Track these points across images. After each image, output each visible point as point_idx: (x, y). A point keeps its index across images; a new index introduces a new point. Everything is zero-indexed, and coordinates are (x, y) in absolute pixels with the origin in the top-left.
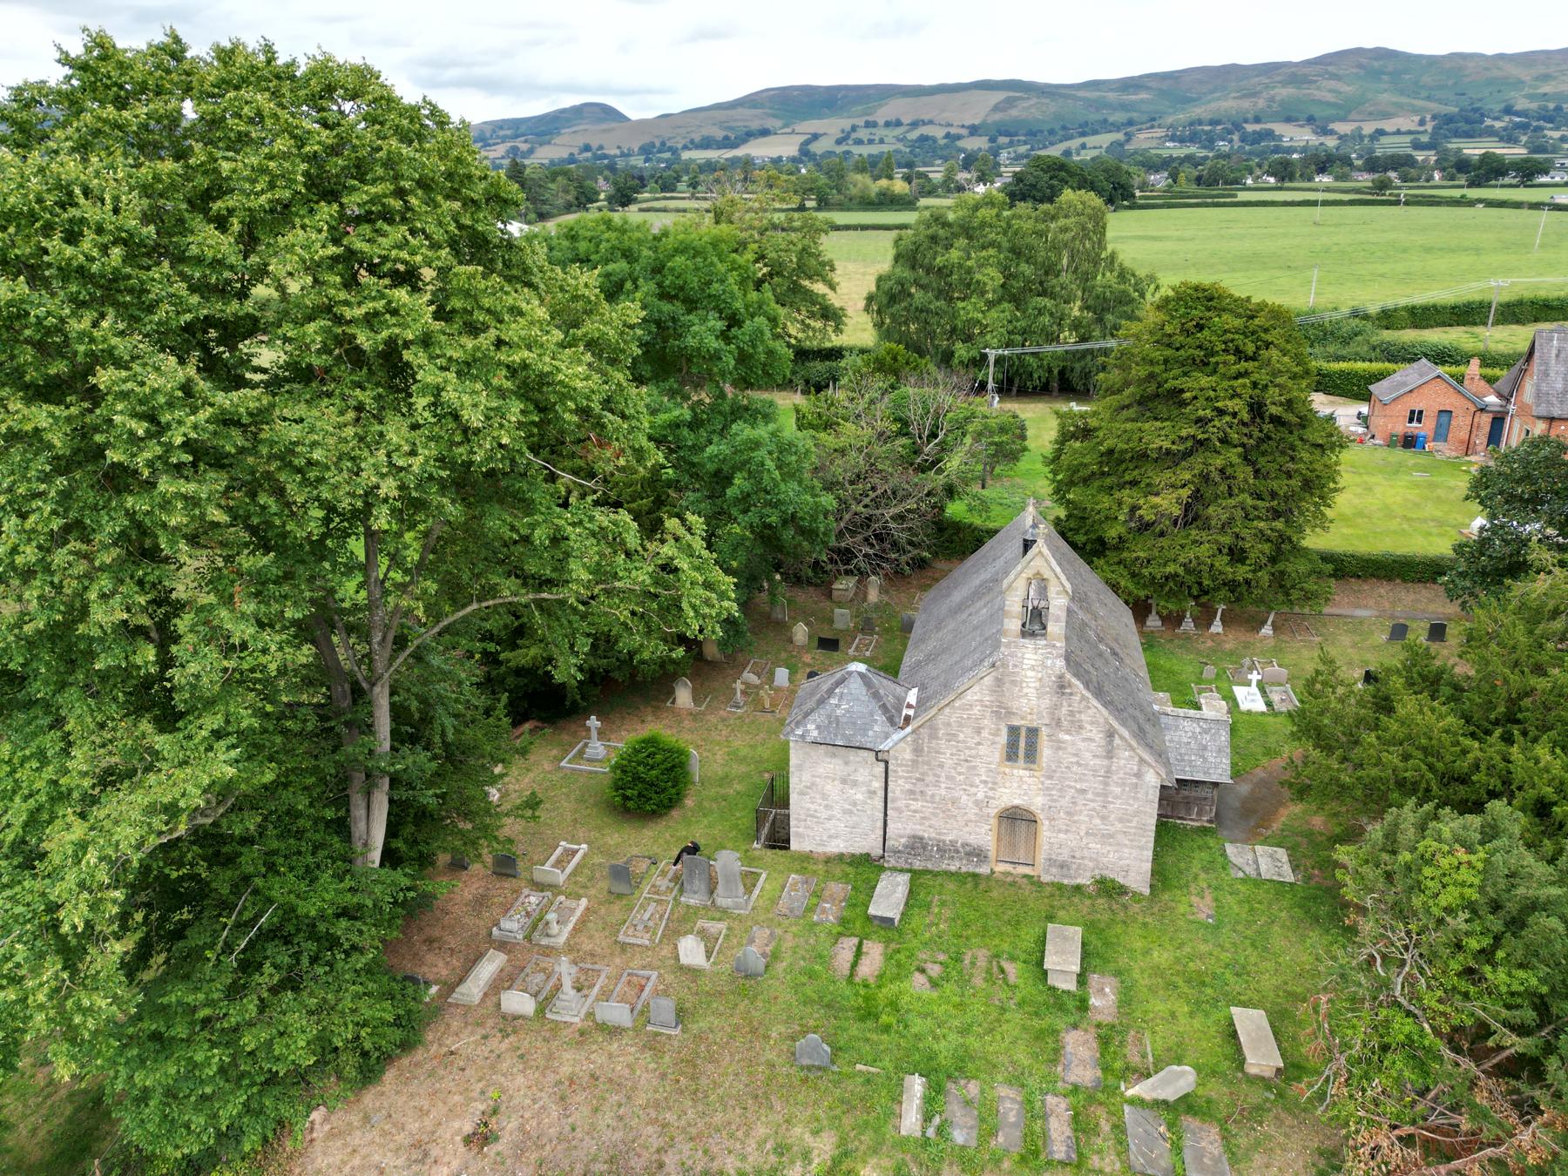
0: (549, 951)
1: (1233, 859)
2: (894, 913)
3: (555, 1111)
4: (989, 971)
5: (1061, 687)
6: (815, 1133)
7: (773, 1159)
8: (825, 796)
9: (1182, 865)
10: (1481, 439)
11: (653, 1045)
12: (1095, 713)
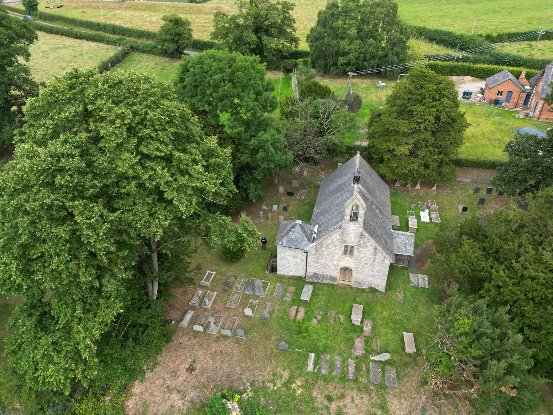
0: (206, 310)
1: (411, 279)
2: (308, 299)
3: (211, 362)
4: (335, 318)
5: (362, 235)
6: (284, 370)
7: (272, 377)
8: (288, 260)
9: (396, 281)
10: (521, 102)
11: (238, 342)
12: (371, 242)
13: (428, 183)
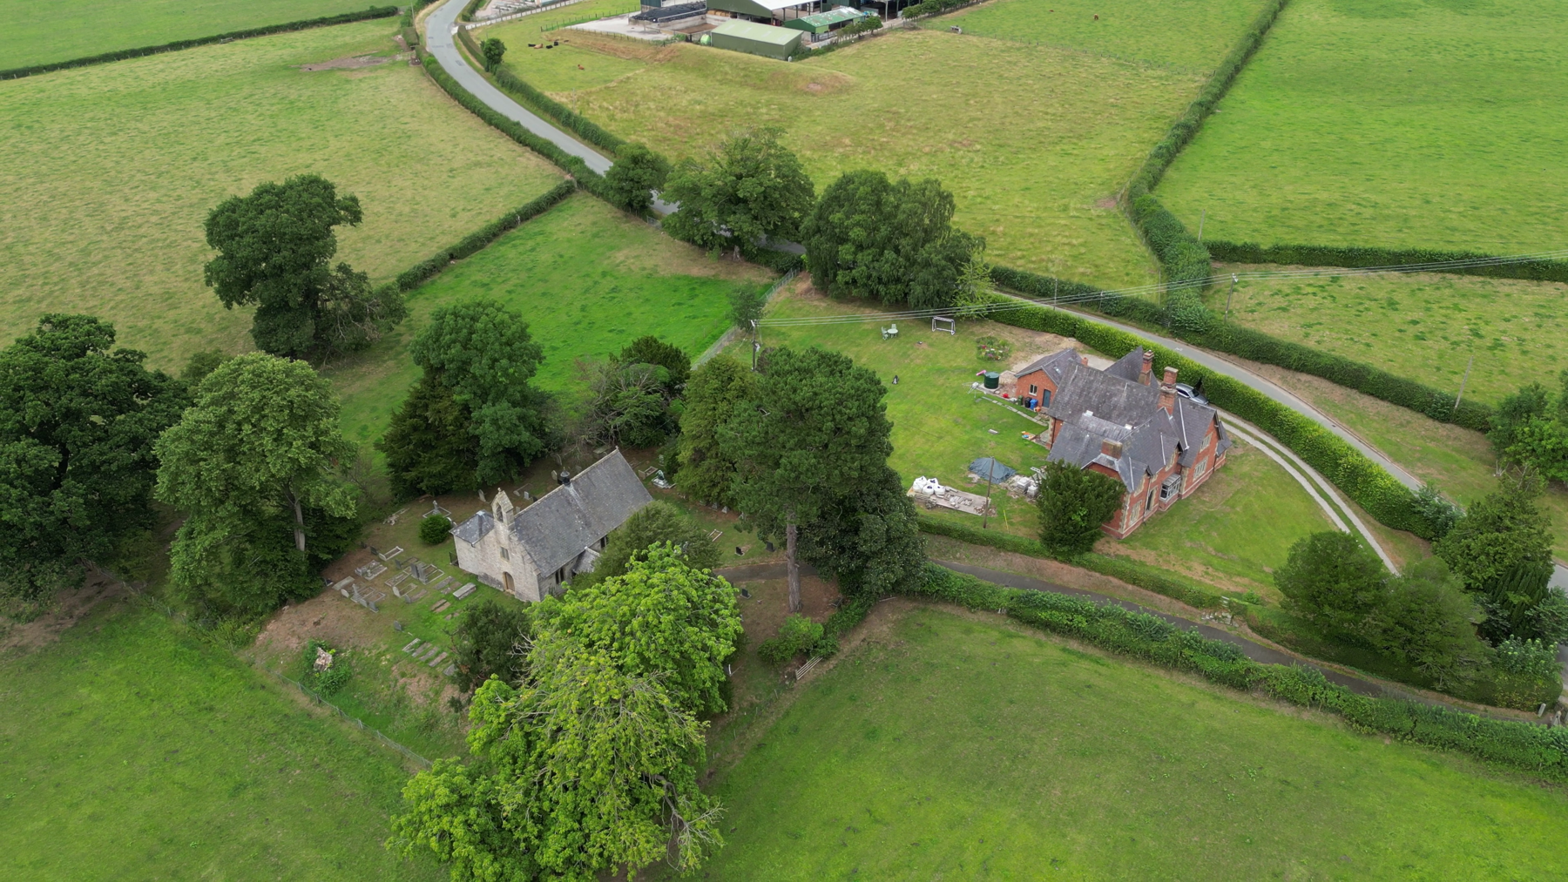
11: (368, 613)
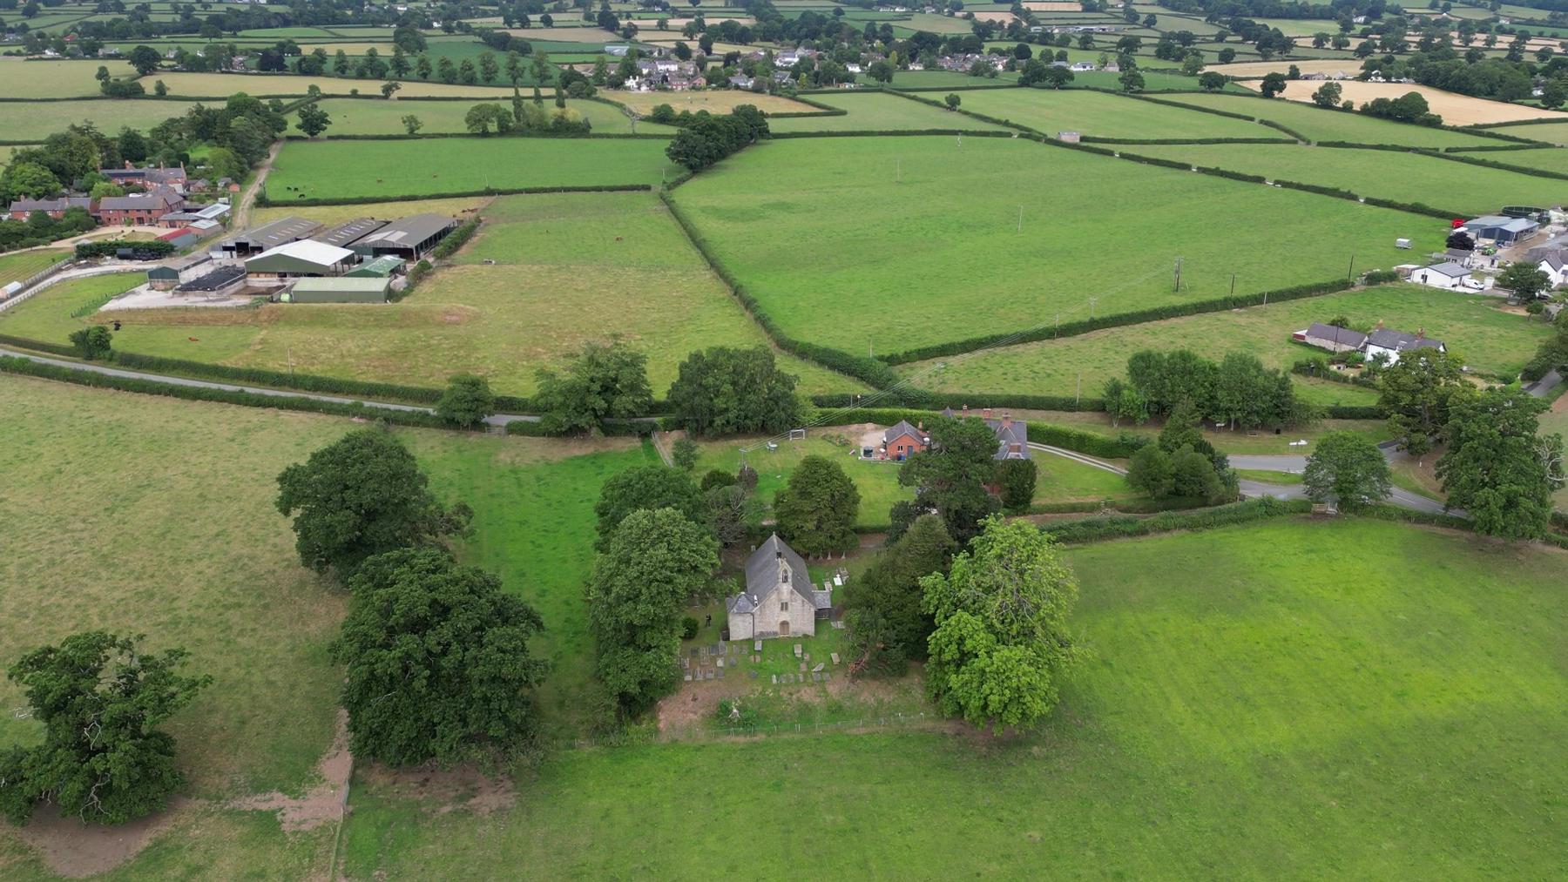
13: (837, 554)
